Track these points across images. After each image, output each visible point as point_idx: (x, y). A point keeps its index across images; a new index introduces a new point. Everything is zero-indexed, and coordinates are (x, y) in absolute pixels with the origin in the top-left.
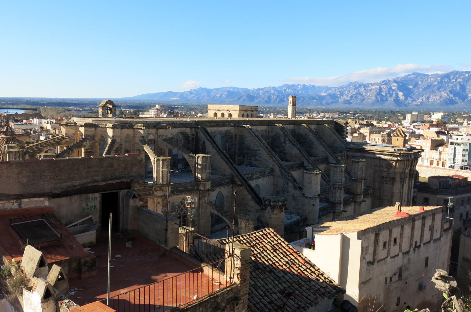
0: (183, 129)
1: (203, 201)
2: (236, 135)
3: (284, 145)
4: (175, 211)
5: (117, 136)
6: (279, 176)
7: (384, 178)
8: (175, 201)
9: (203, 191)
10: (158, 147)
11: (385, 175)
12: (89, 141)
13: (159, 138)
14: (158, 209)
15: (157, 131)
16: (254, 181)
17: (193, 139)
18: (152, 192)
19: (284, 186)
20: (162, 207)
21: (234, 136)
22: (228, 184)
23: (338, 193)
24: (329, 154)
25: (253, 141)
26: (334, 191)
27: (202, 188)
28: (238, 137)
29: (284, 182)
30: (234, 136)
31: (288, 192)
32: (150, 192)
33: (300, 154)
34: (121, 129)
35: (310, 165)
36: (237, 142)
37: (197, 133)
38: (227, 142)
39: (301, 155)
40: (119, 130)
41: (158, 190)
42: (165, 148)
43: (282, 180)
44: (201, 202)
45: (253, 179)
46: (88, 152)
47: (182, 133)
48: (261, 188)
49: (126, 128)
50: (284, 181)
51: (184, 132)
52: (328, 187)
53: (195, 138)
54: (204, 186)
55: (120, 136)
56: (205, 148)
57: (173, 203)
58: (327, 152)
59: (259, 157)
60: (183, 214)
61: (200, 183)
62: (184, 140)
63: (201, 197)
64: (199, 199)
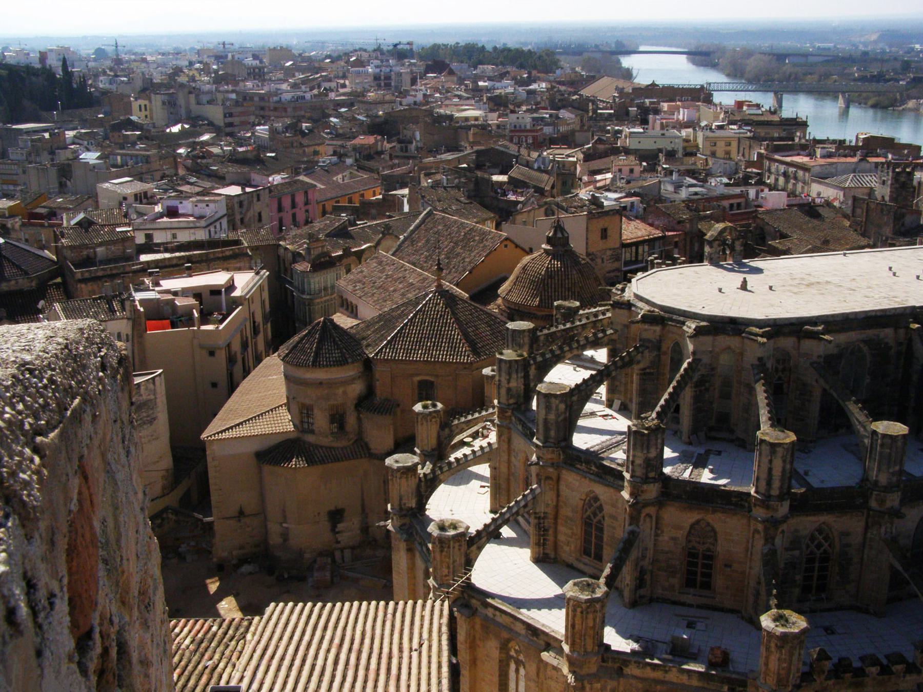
9: (873, 510)
12: (649, 352)
13: (801, 359)
15: (799, 342)
18: (746, 505)
20: (762, 542)
27: (873, 504)
32: (743, 503)
41: (759, 506)
42: (814, 383)
44: (869, 535)
46: (644, 374)
49: (726, 334)
54: (882, 502)
55: (711, 352)
57: (796, 531)
60: (821, 554)
61: (871, 493)
64: (867, 528)
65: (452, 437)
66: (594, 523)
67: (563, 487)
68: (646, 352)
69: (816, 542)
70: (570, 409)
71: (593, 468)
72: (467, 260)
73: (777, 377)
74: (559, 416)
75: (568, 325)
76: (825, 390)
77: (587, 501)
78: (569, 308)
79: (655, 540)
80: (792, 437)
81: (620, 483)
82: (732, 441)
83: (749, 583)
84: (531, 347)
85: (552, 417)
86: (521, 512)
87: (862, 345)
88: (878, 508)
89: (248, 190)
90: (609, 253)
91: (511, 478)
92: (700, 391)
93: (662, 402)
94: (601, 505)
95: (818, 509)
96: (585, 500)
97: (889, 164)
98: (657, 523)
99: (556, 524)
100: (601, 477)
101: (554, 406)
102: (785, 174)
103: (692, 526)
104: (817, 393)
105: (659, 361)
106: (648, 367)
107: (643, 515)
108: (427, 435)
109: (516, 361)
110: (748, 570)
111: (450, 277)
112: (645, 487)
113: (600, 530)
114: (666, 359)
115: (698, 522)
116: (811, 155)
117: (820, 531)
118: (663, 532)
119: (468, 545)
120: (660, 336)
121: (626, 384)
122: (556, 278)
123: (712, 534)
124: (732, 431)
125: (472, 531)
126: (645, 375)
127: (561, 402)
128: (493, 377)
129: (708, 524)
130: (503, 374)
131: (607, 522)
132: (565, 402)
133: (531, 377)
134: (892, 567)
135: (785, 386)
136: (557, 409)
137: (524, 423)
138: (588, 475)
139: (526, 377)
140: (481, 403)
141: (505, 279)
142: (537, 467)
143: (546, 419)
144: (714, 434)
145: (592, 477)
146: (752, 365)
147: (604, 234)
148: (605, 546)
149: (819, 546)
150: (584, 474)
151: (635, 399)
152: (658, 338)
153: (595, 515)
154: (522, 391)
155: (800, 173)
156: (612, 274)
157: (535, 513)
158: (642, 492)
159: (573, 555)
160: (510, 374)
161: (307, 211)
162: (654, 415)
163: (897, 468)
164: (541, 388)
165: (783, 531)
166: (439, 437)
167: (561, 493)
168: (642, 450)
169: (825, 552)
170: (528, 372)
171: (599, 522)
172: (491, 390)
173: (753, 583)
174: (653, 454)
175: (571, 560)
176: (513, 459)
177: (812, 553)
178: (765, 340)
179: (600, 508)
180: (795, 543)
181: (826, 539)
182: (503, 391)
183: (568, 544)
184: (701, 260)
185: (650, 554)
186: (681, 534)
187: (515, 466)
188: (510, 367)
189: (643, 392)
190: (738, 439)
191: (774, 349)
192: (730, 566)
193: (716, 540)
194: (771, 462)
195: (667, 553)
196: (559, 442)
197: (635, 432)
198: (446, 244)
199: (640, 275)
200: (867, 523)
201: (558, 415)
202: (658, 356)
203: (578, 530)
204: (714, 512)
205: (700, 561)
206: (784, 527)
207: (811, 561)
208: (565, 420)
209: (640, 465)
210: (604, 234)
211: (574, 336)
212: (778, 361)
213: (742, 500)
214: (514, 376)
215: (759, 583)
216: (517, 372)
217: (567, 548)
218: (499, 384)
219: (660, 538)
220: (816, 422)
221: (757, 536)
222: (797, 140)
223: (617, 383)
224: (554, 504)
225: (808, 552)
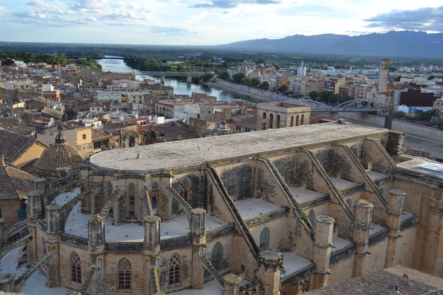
1: (196, 255)
2: (255, 168)
3: (311, 173)
4: (166, 265)
5: (121, 186)
6: (293, 218)
7: (432, 207)
8: (166, 257)
10: (162, 194)
11: (433, 205)
13: (162, 186)
14: (147, 265)
15: (161, 179)
16: (262, 225)
17: (202, 180)
19: (297, 229)
20: (150, 264)
21: (253, 169)
22: (227, 234)
23: (362, 234)
24: (366, 181)
25: (270, 177)
26: (358, 231)
28: (257, 170)
29: (297, 225)
30: (253, 169)
31: (301, 236)
32: (141, 249)
33: (326, 186)
34: (126, 178)
35: (336, 199)
36: (256, 175)
37: (206, 175)
38: (244, 176)
39: (328, 187)
40: (124, 180)
43: (296, 222)
44: (194, 256)
47: (189, 176)
48: (271, 230)
50: (297, 223)
51: (192, 175)
52: (352, 225)
53: (204, 179)
55: (124, 186)
56: (213, 191)
58: (364, 178)
59: (275, 194)
62: (192, 182)
63: (194, 251)
64: (193, 253)
66: (76, 266)
67: (61, 252)
68: (97, 188)
69: (173, 262)
70: (63, 216)
71: (74, 241)
72: (19, 151)
73: (153, 194)
74: (57, 219)
76: (173, 198)
77: (72, 256)
79: (104, 270)
81: (87, 246)
82: (136, 223)
83: (146, 283)
85: (54, 220)
86: (42, 265)
87: (187, 178)
88: (197, 244)
91: (38, 250)
92: (121, 203)
94: (79, 257)
95: (172, 248)
96: (71, 256)
98: (104, 262)
99: (59, 269)
100: (78, 245)
101: (54, 215)
103: (120, 262)
104: (170, 200)
105: (103, 191)
106: (98, 194)
107: (97, 260)
109: (37, 196)
110: (145, 278)
112: (97, 247)
113: (79, 269)
114: (106, 190)
115: (122, 259)
117: (174, 257)
118: (107, 266)
119: (15, 284)
120: (102, 180)
121: (89, 202)
122: (60, 157)
123: (129, 264)
124: (136, 219)
125: (16, 278)
127: (58, 213)
129: (127, 260)
131: (81, 265)
132: (60, 213)
133: (45, 203)
134: (204, 268)
135: (157, 197)
136: (56, 217)
137: (42, 224)
138: (72, 245)
139: (42, 203)
142: (48, 243)
143: (51, 221)
144: (128, 220)
145: (74, 245)
146: (142, 190)
148: (82, 276)
149: (174, 263)
150: (70, 244)
151: (93, 209)
152: (101, 181)
153: (77, 262)
154: (41, 210)
157: (49, 265)
158: (96, 249)
159: (68, 282)
160: (34, 202)
163: (203, 227)
165: (158, 259)
167: (60, 254)
168: (95, 230)
170: (43, 201)
173: (148, 283)
175: (67, 284)
176: (38, 241)
177: (172, 266)
179: (79, 259)
180: (164, 264)
183: (65, 277)
186: (115, 266)
187: (39, 244)
188: (34, 199)
189: (96, 205)
190: (139, 222)
191: (151, 182)
192: (138, 277)
193: (131, 267)
194: (150, 230)
195: (110, 275)
196: (58, 231)
197: (91, 223)
200: (193, 251)
202: (102, 189)
203: (69, 270)
205: (125, 277)
206: (159, 257)
207: (172, 270)
208: (60, 220)
209: (94, 238)
212: (153, 187)
213: (140, 247)
215: (150, 283)
216: (38, 201)
217: (65, 279)
218: (30, 207)
219: (106, 269)
220: (171, 211)
221: (147, 262)
223: (85, 202)
224: (58, 259)
225: (170, 266)
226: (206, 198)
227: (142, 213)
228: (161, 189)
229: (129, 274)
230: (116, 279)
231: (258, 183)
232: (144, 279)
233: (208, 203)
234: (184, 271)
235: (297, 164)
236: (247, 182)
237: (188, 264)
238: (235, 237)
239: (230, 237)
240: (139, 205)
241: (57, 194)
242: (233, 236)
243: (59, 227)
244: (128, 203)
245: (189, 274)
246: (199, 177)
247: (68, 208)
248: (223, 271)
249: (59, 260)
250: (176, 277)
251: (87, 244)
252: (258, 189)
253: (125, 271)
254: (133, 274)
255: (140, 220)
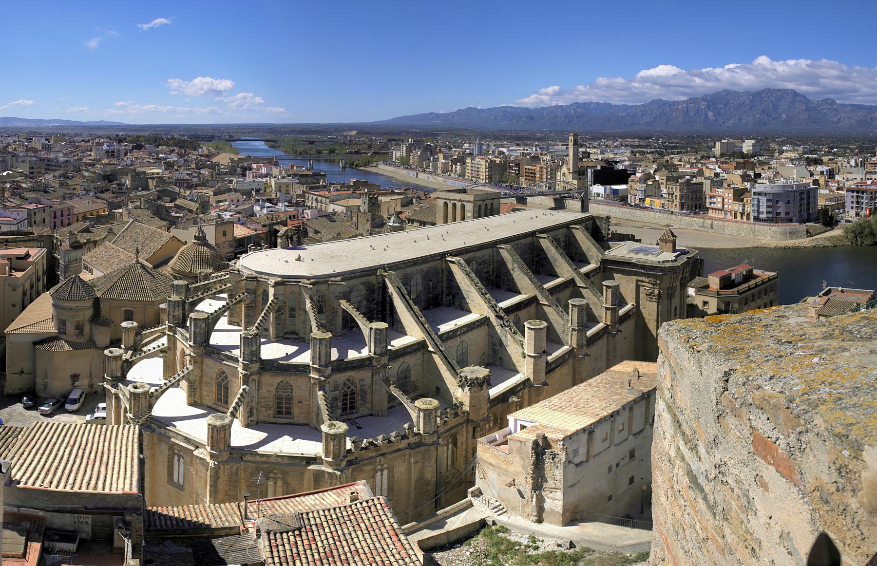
0: (365, 279)
45: (456, 336)
62: (367, 290)
65: (142, 340)
75: (206, 282)
78: (207, 273)
80: (329, 335)
84: (186, 294)
85: (198, 330)
89: (39, 206)
90: (227, 243)
93: (258, 321)
97: (366, 193)
102: (317, 200)
103: (278, 384)
108: (127, 339)
111: (143, 256)
115: (281, 382)
116: (329, 191)
124: (297, 334)
126: (248, 307)
128: (165, 309)
130: (171, 308)
139: (184, 309)
140: (158, 323)
141: (172, 257)
144: (287, 336)
147: (224, 234)
149: (349, 388)
155: (324, 199)
156: (229, 254)
161: (69, 219)
162: (254, 328)
164: (192, 315)
166: (135, 340)
169: (352, 390)
171: (226, 384)
172: (164, 316)
174: (254, 348)
177: (345, 391)
178: (311, 286)
179: (226, 377)
181: (352, 384)
182: (171, 317)
184: (276, 246)
185: (255, 399)
198: (141, 239)
199: (244, 255)
201: (201, 329)
204: (290, 376)
207: (345, 395)
208: (205, 332)
210: (224, 234)
211: (209, 288)
212: (319, 297)
214: (177, 309)
222: (321, 183)
226: (384, 309)
227: (305, 327)
228: (328, 299)
229: (290, 399)
230: (272, 403)
231: (447, 288)
232: (309, 405)
233: (388, 315)
234: (362, 396)
235: (493, 262)
236: (435, 288)
237: (365, 388)
238: (425, 355)
239: (419, 355)
240: (302, 318)
241: (201, 300)
242: (423, 354)
243: (203, 340)
244: (288, 315)
245: (368, 400)
246: (375, 283)
247: (214, 318)
248: (412, 395)
249: (202, 376)
250: (351, 403)
251: (238, 361)
252: (448, 295)
253: (284, 395)
254: (295, 399)
255: (303, 336)
